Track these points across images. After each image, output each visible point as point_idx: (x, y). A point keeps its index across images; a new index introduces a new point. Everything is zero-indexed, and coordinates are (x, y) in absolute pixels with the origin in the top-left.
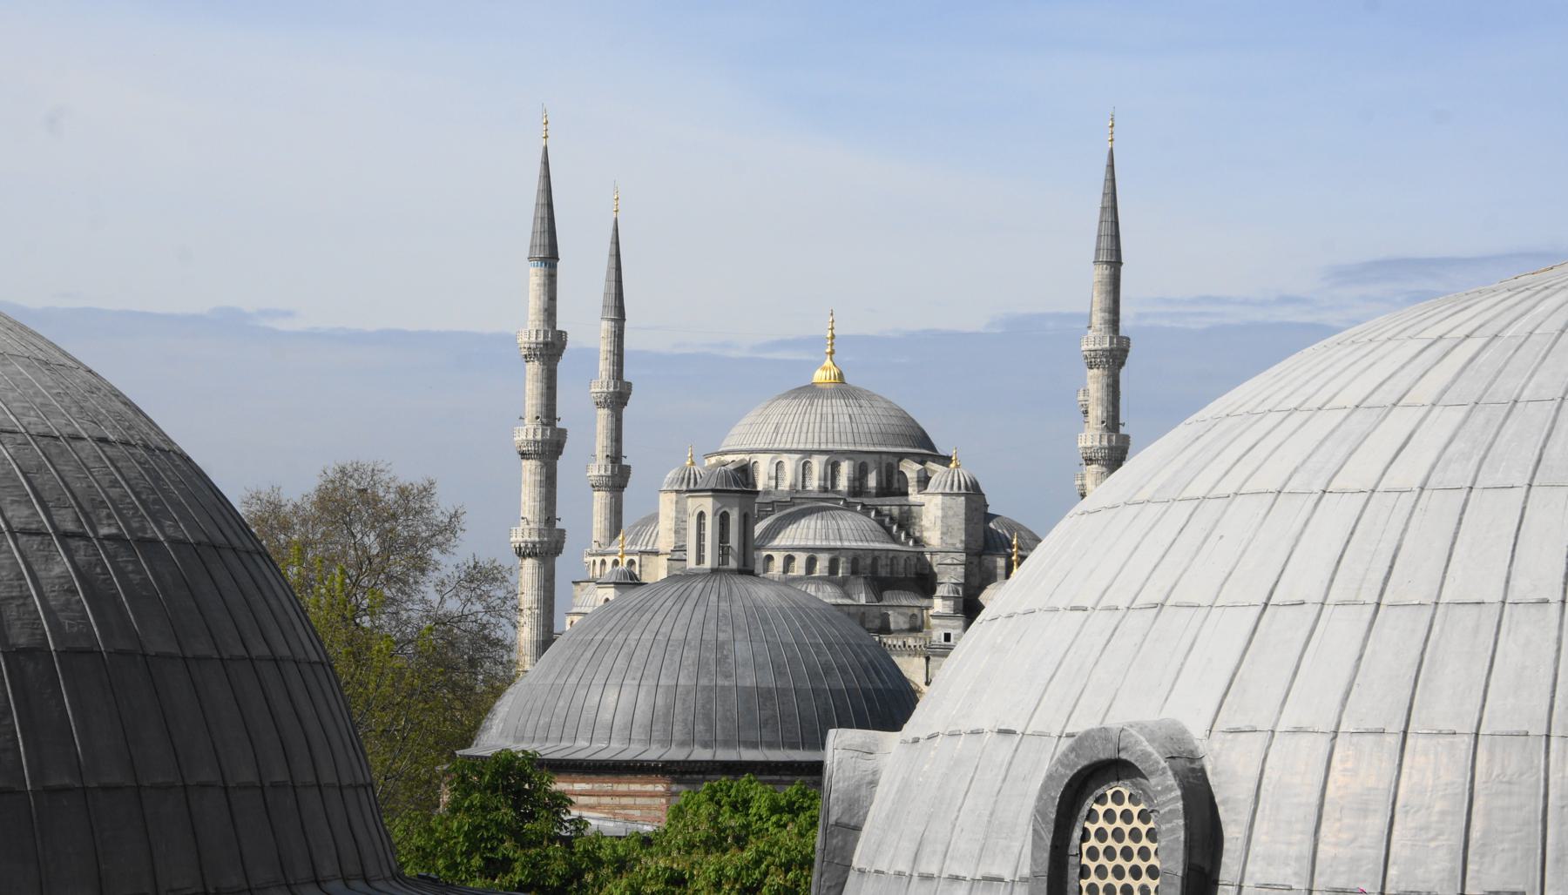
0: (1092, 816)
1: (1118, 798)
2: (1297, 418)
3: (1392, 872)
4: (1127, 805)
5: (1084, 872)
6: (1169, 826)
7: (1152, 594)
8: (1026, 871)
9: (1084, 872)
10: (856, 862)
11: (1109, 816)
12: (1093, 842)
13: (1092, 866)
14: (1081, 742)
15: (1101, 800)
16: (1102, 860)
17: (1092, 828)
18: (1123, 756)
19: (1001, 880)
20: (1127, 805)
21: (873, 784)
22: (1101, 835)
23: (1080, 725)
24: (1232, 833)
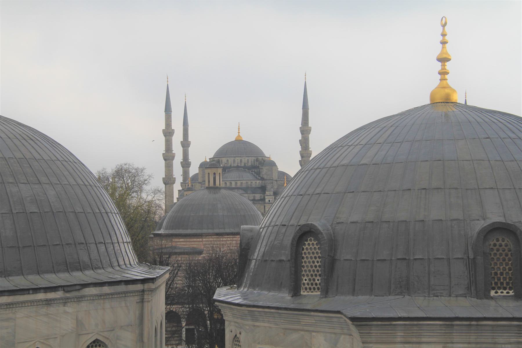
0: (305, 244)
1: (311, 240)
4: (313, 242)
5: (303, 258)
8: (289, 258)
9: (303, 258)
11: (309, 244)
12: (305, 251)
13: (305, 257)
15: (307, 241)
16: (307, 255)
17: (305, 248)
18: (312, 230)
20: (313, 242)
22: (307, 249)
23: (302, 222)
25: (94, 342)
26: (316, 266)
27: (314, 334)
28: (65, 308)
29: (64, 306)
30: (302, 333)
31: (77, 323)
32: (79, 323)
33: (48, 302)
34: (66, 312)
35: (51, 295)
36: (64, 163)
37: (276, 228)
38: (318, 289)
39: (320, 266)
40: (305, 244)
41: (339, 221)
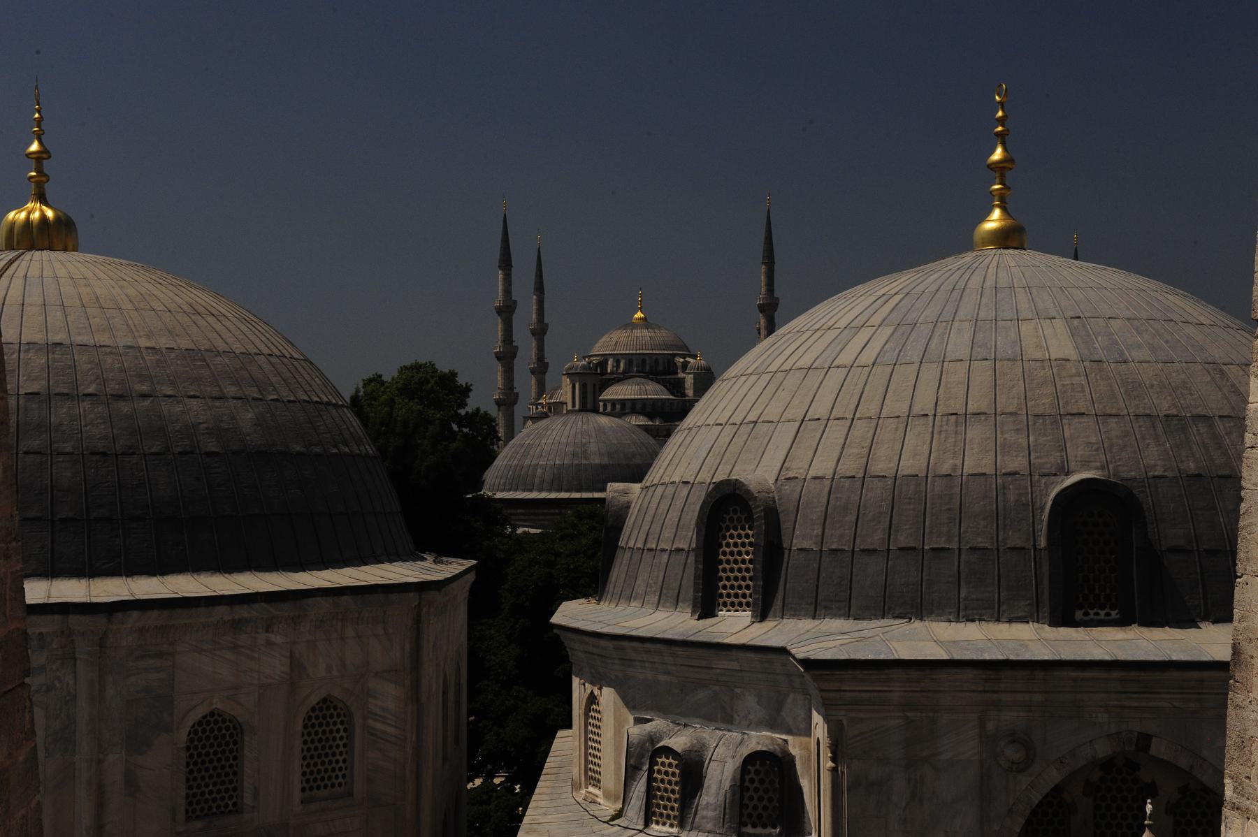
0: (723, 520)
1: (735, 512)
2: (820, 333)
3: (858, 541)
6: (758, 523)
7: (752, 417)
8: (694, 545)
10: (622, 543)
14: (719, 485)
18: (737, 492)
19: (683, 550)
21: (628, 507)
23: (720, 477)
24: (786, 525)
25: (324, 700)
26: (744, 562)
27: (738, 690)
28: (270, 635)
29: (267, 631)
30: (716, 688)
31: (291, 663)
32: (295, 664)
33: (237, 625)
34: (269, 643)
35: (243, 612)
36: (273, 360)
37: (671, 489)
38: (748, 604)
39: (751, 561)
40: (723, 520)
41: (791, 474)
